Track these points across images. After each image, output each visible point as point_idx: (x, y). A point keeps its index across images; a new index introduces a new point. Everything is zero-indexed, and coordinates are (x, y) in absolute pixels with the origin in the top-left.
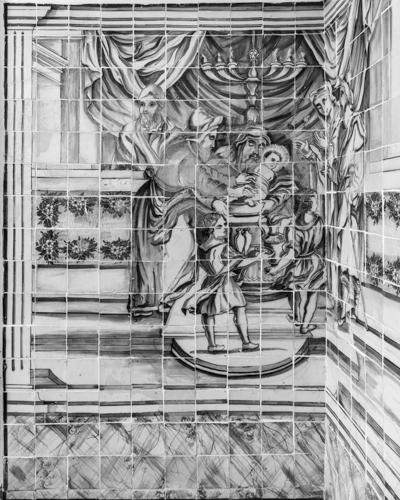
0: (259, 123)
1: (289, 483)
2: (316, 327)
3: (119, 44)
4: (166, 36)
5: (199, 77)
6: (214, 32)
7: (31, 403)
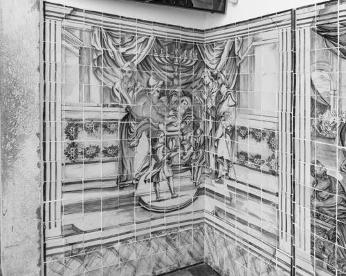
1: (191, 258)
2: (201, 183)
3: (112, 37)
4: (137, 36)
5: (152, 60)
6: (159, 38)
7: (62, 246)
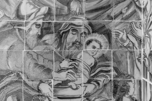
0: (81, 14)
